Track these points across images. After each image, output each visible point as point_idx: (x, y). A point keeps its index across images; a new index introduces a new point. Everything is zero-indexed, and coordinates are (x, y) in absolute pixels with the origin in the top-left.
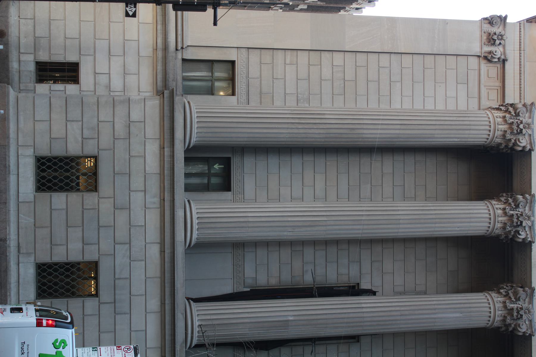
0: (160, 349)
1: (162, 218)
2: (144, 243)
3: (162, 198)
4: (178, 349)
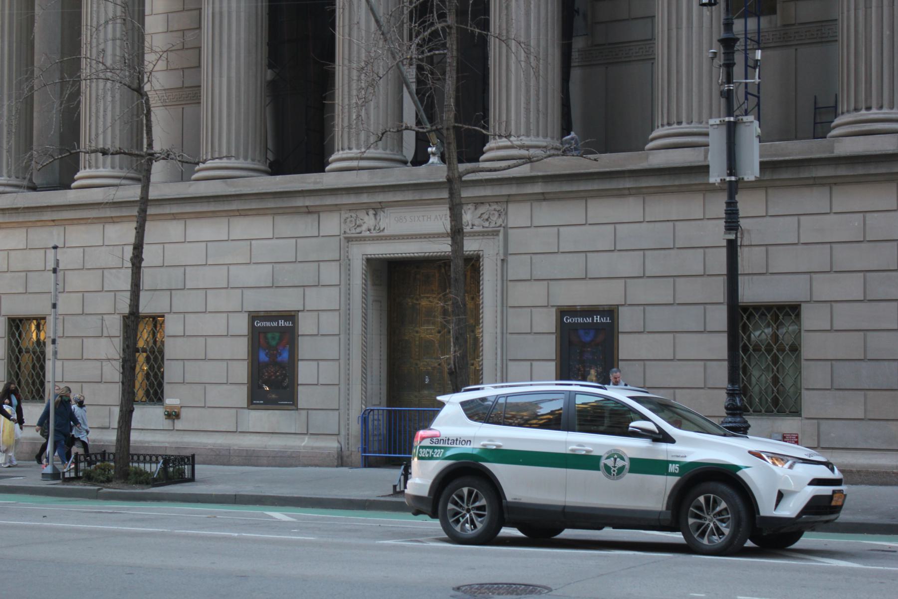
0: (231, 219)
1: (75, 222)
2: (103, 248)
3: (52, 223)
4: (234, 190)
